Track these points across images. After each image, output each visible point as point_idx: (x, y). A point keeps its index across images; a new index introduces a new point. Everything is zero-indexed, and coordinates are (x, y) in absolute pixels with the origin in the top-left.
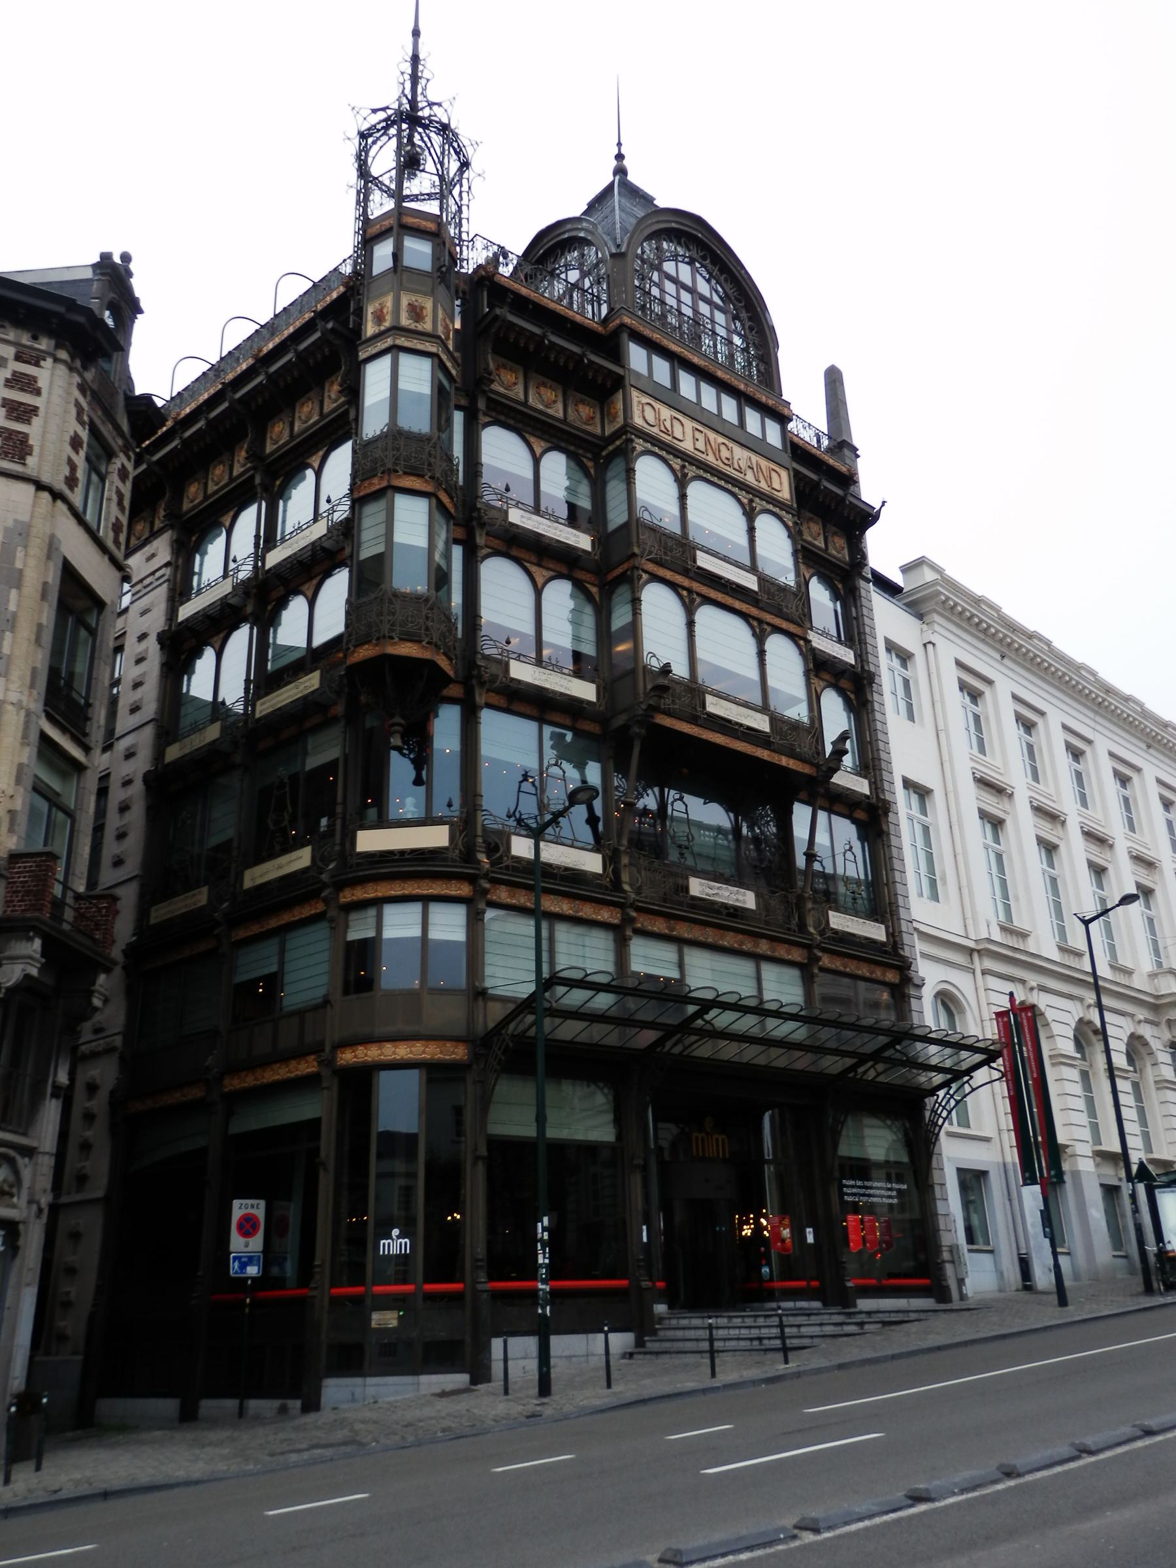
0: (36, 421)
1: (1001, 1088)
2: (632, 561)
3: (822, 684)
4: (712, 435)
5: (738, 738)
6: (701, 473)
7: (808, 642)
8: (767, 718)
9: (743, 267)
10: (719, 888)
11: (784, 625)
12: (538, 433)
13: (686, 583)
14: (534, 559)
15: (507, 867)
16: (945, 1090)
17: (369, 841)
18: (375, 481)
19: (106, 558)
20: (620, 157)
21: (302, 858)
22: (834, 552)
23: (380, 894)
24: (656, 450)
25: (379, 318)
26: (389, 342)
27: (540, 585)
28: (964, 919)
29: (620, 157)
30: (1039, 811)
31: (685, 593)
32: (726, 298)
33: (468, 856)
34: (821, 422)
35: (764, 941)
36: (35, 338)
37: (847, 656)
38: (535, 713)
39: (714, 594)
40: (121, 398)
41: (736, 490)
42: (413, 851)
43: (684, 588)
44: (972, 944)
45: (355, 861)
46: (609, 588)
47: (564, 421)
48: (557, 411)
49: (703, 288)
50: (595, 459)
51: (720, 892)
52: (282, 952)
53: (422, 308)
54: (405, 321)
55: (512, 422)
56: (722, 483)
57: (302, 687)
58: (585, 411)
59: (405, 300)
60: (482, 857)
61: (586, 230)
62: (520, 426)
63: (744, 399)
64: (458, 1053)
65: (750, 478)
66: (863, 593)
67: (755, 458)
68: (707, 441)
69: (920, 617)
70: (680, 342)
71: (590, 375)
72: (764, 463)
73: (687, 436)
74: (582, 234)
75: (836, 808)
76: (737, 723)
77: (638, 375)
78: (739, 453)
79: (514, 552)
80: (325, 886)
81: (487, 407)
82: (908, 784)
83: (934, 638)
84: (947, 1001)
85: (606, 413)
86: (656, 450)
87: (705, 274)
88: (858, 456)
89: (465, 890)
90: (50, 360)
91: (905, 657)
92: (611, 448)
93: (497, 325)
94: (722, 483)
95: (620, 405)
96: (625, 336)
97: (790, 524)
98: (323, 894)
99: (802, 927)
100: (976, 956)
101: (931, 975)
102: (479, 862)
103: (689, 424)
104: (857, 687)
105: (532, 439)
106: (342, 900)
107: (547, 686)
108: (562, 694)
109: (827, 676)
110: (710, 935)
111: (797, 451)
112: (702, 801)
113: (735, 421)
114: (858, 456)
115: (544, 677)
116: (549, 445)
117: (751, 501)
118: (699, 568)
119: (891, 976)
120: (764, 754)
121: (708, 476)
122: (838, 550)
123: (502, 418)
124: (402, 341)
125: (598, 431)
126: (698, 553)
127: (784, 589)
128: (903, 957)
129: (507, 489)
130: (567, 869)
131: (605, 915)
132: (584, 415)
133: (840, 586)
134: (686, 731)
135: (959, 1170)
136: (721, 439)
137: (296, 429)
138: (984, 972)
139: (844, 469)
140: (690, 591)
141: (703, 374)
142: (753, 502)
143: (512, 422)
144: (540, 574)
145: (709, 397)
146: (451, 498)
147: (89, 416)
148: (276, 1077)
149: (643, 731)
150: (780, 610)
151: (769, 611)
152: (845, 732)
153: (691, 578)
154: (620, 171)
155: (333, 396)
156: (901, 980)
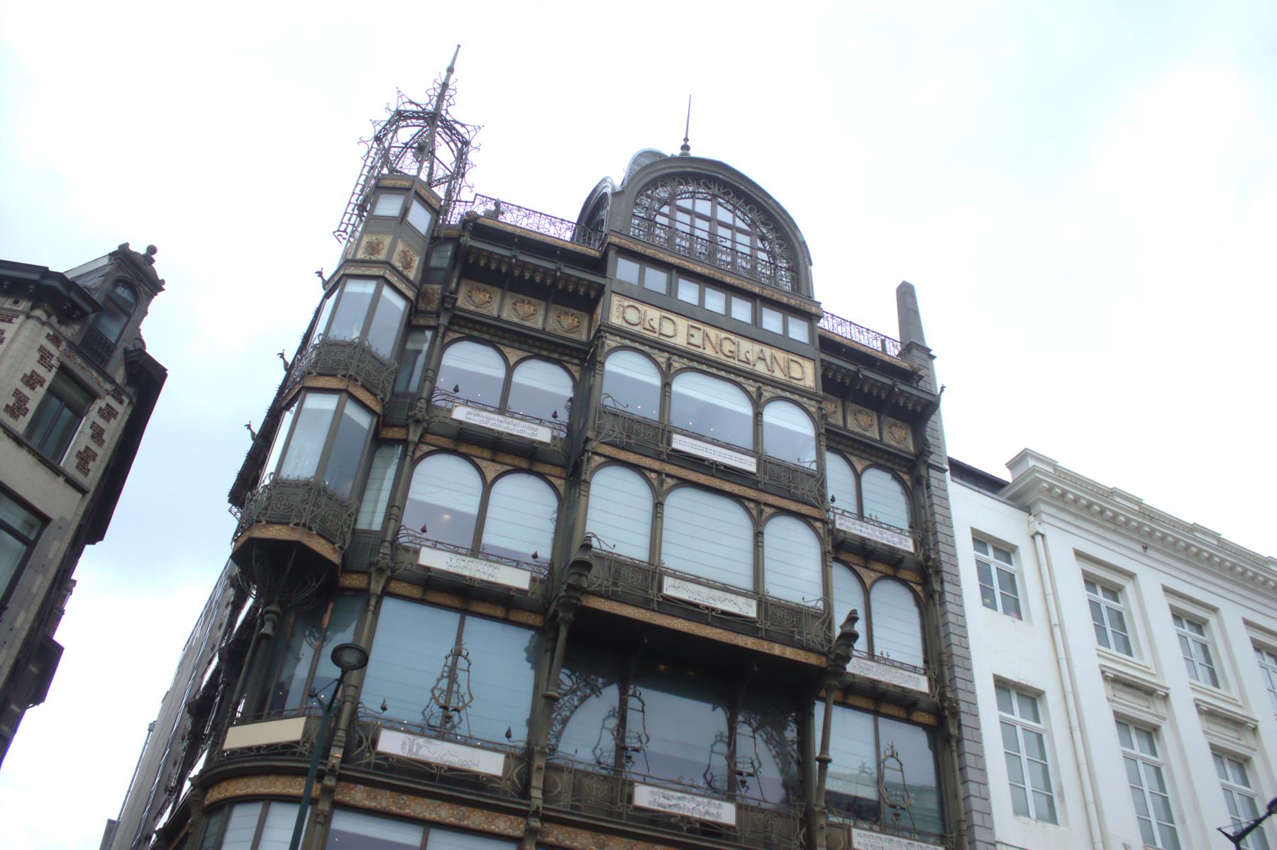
3: (874, 575)
4: (712, 333)
5: (708, 624)
6: (695, 365)
7: (824, 522)
8: (754, 603)
9: (770, 197)
10: (679, 798)
11: (793, 506)
12: (516, 345)
13: (656, 465)
14: (486, 454)
15: (368, 765)
17: (240, 737)
19: (61, 480)
22: (893, 443)
23: (228, 794)
24: (637, 345)
27: (489, 480)
30: (1210, 714)
31: (653, 475)
32: (753, 224)
34: (893, 331)
36: (16, 302)
37: (907, 545)
38: (457, 603)
39: (693, 476)
40: (119, 353)
41: (741, 380)
42: (269, 746)
43: (652, 470)
47: (543, 331)
51: (681, 803)
53: (378, 244)
55: (486, 337)
56: (723, 374)
58: (568, 321)
62: (495, 339)
63: (760, 300)
65: (761, 368)
66: (933, 482)
67: (768, 351)
69: (1027, 509)
70: (701, 263)
71: (571, 288)
72: (781, 356)
73: (679, 332)
75: (885, 709)
76: (707, 608)
77: (622, 282)
78: (746, 345)
79: (463, 449)
81: (450, 323)
82: (1002, 685)
86: (637, 345)
87: (730, 207)
88: (934, 357)
90: (22, 317)
91: (1006, 551)
94: (723, 374)
96: (612, 254)
97: (813, 410)
103: (682, 324)
104: (923, 575)
105: (507, 350)
107: (465, 573)
108: (482, 581)
109: (883, 568)
111: (829, 344)
112: (710, 706)
114: (934, 357)
115: (463, 564)
116: (526, 354)
117: (759, 388)
118: (674, 450)
120: (749, 642)
121: (704, 367)
122: (898, 438)
123: (476, 334)
125: (584, 338)
126: (676, 437)
127: (794, 472)
129: (456, 390)
130: (451, 769)
131: (501, 824)
132: (565, 324)
133: (906, 477)
134: (631, 616)
136: (724, 335)
140: (659, 473)
141: (705, 281)
142: (761, 389)
143: (486, 337)
144: (491, 470)
145: (715, 301)
146: (375, 395)
147: (58, 359)
151: (770, 491)
152: (854, 612)
153: (663, 461)
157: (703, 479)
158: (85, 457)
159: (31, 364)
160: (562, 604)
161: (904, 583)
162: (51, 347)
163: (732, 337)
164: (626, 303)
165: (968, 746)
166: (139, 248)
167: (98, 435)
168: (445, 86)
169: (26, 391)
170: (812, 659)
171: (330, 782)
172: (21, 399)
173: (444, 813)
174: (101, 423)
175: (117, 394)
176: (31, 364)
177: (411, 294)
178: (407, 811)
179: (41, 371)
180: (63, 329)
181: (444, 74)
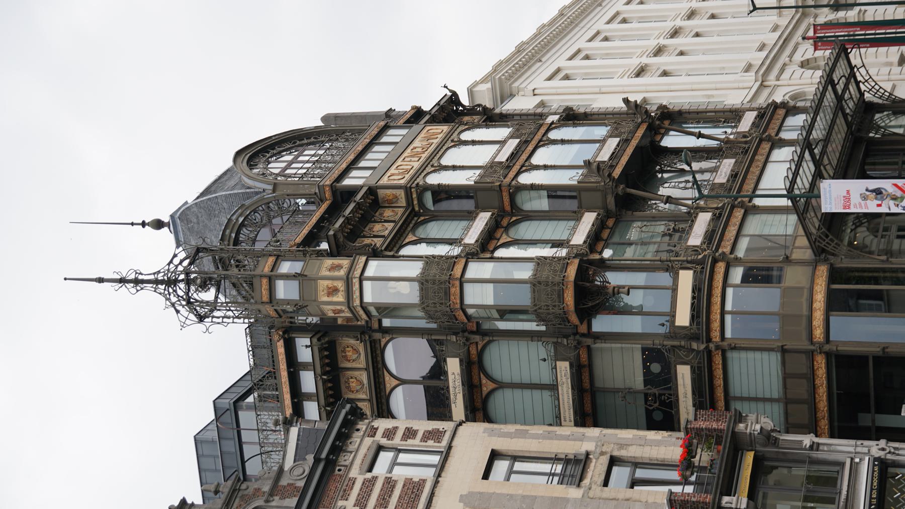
0: (415, 428)
1: (863, 50)
2: (503, 188)
16: (861, 84)
17: (683, 318)
18: (453, 290)
20: (143, 224)
21: (684, 373)
23: (719, 311)
25: (333, 291)
26: (356, 282)
28: (739, 88)
29: (143, 224)
33: (702, 262)
35: (756, 157)
41: (444, 148)
42: (693, 291)
44: (758, 83)
45: (695, 326)
46: (515, 208)
48: (390, 226)
49: (289, 158)
50: (418, 215)
52: (742, 399)
54: (342, 273)
57: (564, 380)
59: (325, 273)
60: (700, 257)
61: (240, 215)
62: (398, 246)
64: (823, 271)
65: (435, 141)
68: (411, 156)
72: (422, 135)
74: (241, 220)
78: (417, 143)
80: (707, 347)
83: (531, 87)
84: (794, 97)
85: (391, 203)
89: (721, 267)
92: (415, 202)
93: (340, 235)
94: (440, 153)
95: (389, 192)
98: (713, 349)
99: (746, 142)
100: (765, 83)
101: (779, 100)
102: (705, 256)
103: (399, 162)
105: (407, 240)
106: (718, 339)
113: (393, 147)
119: (782, 112)
120: (634, 143)
124: (357, 273)
126: (496, 160)
128: (768, 105)
136: (409, 150)
137: (364, 397)
138: (778, 79)
140: (523, 166)
148: (825, 398)
149: (622, 186)
154: (158, 224)
155: (355, 356)
156: (784, 108)
160: (616, 187)
164: (385, 178)
165: (686, 107)
168: (123, 281)
170: (640, 133)
178: (733, 239)
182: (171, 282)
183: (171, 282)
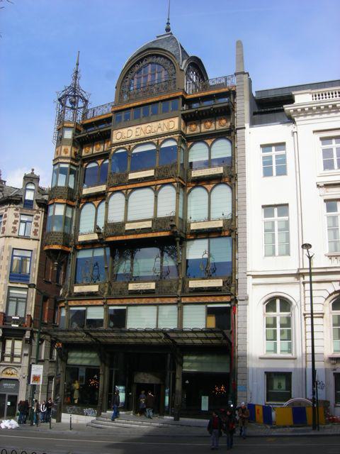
3: (212, 186)
11: (166, 181)
20: (168, 24)
22: (221, 128)
29: (168, 24)
40: (35, 202)
56: (148, 141)
65: (160, 132)
83: (295, 130)
88: (248, 73)
91: (281, 145)
110: (136, 301)
120: (150, 235)
131: (100, 302)
135: (265, 372)
139: (227, 90)
150: (163, 176)
154: (168, 30)
157: (138, 185)
158: (35, 232)
159: (14, 219)
161: (225, 183)
162: (16, 212)
163: (150, 124)
166: (28, 172)
167: (36, 225)
168: (77, 72)
169: (15, 226)
171: (66, 302)
172: (14, 228)
173: (88, 303)
174: (37, 221)
175: (38, 212)
176: (14, 219)
177: (69, 161)
179: (16, 219)
180: (18, 206)
181: (75, 66)
182: (74, 90)
183: (75, 88)
